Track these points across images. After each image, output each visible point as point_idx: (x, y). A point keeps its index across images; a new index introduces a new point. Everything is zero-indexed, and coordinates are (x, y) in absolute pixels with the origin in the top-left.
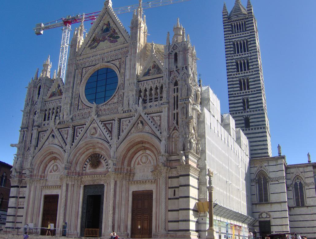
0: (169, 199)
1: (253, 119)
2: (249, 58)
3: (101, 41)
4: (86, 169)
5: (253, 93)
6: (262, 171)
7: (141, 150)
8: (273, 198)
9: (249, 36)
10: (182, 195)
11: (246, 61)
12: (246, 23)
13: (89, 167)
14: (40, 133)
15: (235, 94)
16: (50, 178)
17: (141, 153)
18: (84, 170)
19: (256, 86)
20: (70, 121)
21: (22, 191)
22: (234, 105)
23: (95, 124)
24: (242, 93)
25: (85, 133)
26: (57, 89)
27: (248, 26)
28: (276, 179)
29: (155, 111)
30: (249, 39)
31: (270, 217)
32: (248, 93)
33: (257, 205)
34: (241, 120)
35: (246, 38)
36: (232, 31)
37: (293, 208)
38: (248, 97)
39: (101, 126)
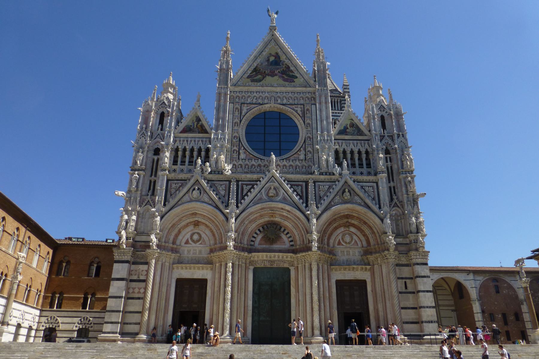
0: (400, 293)
3: (268, 75)
4: (254, 244)
7: (343, 226)
10: (423, 289)
13: (261, 240)
14: (170, 182)
16: (186, 252)
17: (343, 230)
18: (251, 245)
20: (230, 171)
21: (136, 271)
23: (275, 182)
25: (259, 192)
26: (196, 124)
29: (366, 180)
39: (288, 187)
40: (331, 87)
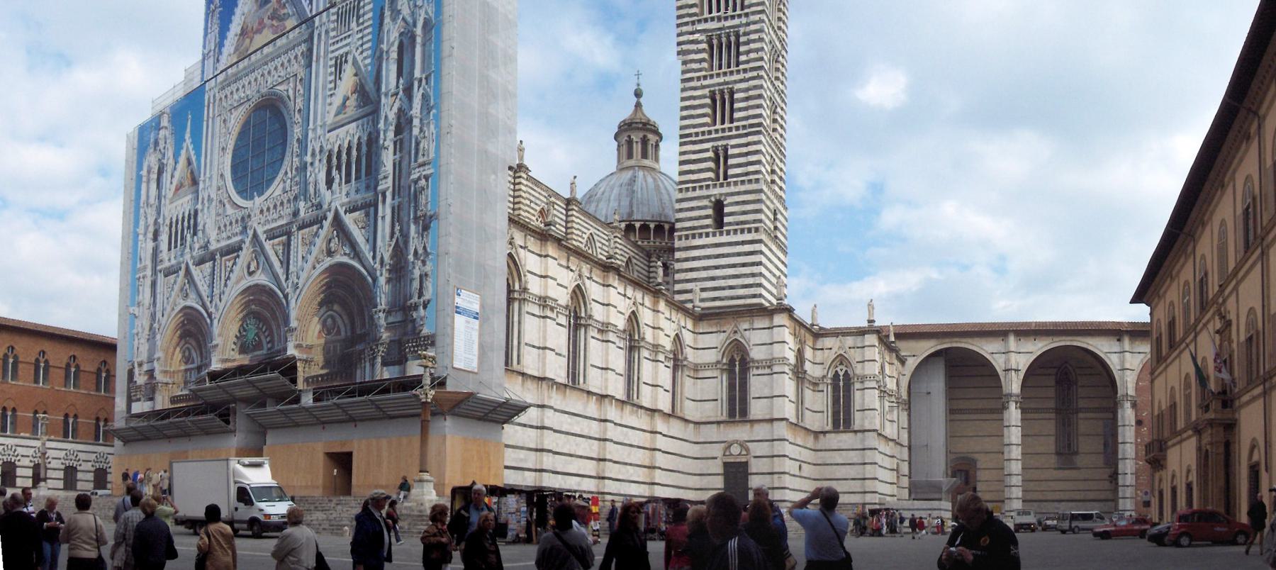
2: (742, 30)
5: (741, 132)
11: (733, 39)
15: (697, 134)
19: (751, 112)
24: (713, 132)
38: (728, 145)
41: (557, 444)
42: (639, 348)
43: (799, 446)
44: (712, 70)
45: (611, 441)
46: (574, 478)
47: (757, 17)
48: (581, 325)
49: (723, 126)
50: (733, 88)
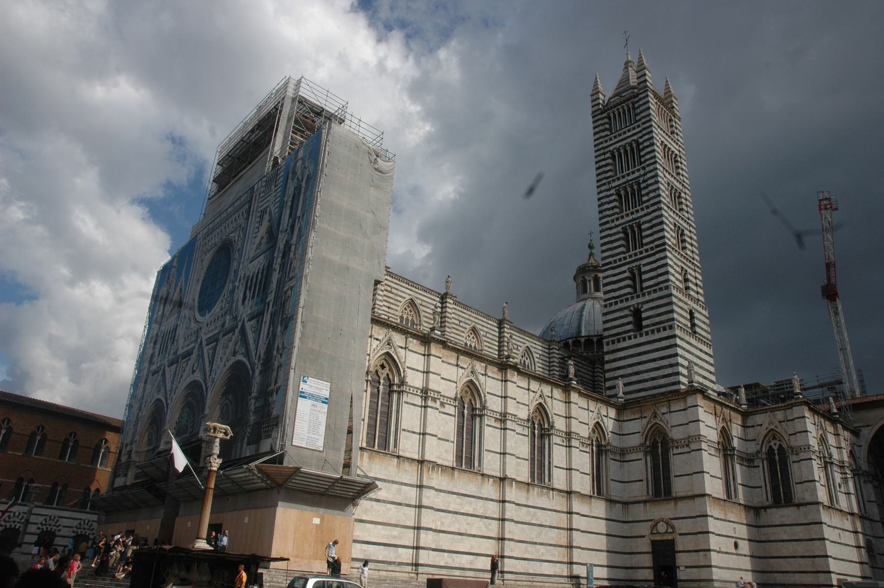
1: (647, 310)
2: (641, 179)
5: (650, 252)
6: (657, 425)
8: (679, 487)
9: (641, 131)
11: (635, 187)
12: (636, 106)
15: (615, 262)
19: (656, 236)
22: (613, 285)
27: (638, 111)
28: (685, 442)
30: (641, 137)
31: (673, 532)
32: (639, 256)
33: (647, 504)
34: (626, 316)
35: (635, 137)
36: (610, 130)
37: (765, 508)
38: (640, 264)
40: (623, 86)
41: (442, 523)
42: (549, 435)
43: (733, 522)
44: (623, 212)
45: (512, 520)
46: (465, 556)
47: (652, 167)
48: (475, 415)
49: (634, 252)
50: (640, 221)
